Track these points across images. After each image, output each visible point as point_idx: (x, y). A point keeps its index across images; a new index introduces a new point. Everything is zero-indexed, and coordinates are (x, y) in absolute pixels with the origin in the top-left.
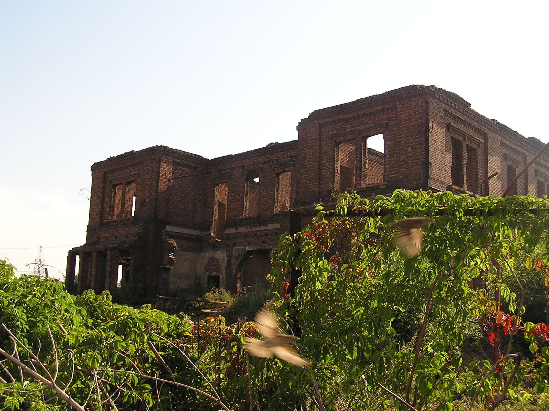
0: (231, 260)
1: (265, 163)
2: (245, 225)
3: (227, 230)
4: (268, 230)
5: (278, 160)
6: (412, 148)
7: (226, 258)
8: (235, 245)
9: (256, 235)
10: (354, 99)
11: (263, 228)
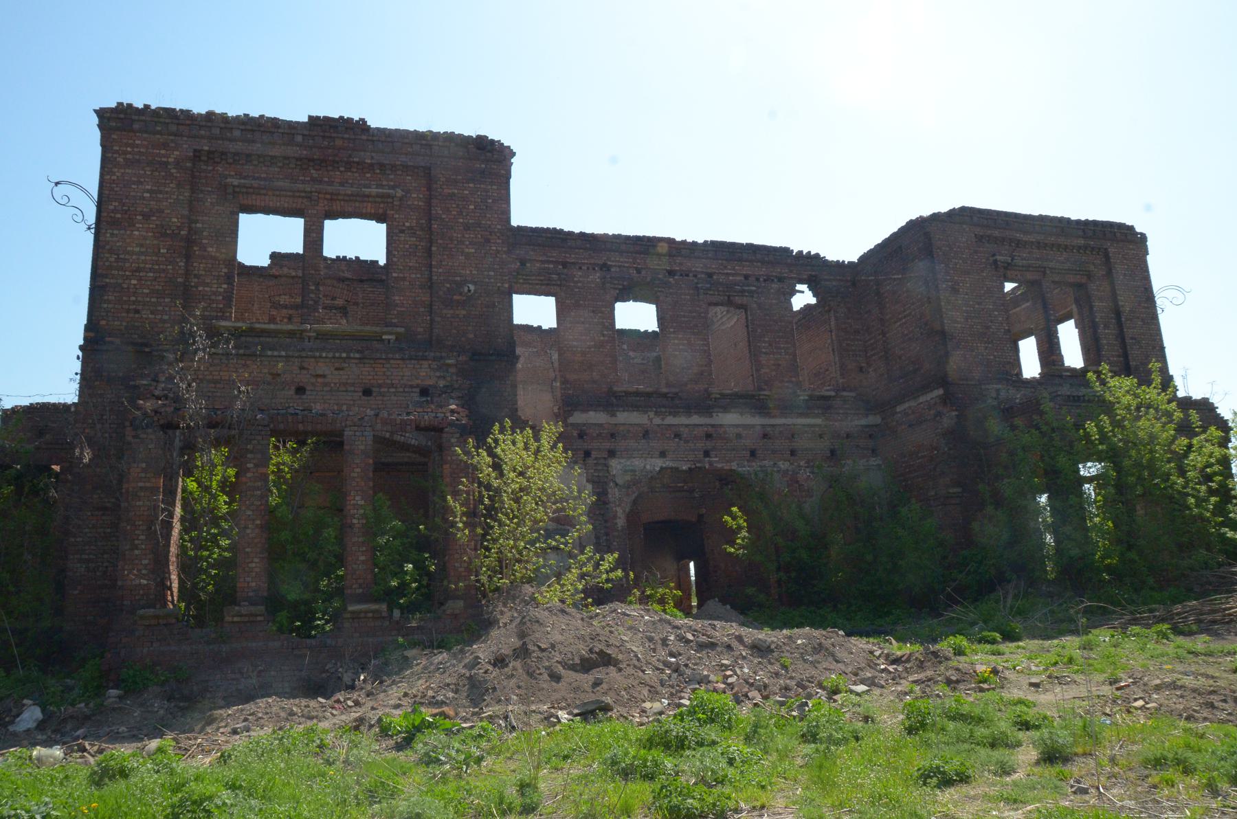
4: (713, 426)
5: (710, 275)
6: (1143, 320)
8: (612, 453)
9: (677, 435)
10: (1036, 212)
11: (696, 419)
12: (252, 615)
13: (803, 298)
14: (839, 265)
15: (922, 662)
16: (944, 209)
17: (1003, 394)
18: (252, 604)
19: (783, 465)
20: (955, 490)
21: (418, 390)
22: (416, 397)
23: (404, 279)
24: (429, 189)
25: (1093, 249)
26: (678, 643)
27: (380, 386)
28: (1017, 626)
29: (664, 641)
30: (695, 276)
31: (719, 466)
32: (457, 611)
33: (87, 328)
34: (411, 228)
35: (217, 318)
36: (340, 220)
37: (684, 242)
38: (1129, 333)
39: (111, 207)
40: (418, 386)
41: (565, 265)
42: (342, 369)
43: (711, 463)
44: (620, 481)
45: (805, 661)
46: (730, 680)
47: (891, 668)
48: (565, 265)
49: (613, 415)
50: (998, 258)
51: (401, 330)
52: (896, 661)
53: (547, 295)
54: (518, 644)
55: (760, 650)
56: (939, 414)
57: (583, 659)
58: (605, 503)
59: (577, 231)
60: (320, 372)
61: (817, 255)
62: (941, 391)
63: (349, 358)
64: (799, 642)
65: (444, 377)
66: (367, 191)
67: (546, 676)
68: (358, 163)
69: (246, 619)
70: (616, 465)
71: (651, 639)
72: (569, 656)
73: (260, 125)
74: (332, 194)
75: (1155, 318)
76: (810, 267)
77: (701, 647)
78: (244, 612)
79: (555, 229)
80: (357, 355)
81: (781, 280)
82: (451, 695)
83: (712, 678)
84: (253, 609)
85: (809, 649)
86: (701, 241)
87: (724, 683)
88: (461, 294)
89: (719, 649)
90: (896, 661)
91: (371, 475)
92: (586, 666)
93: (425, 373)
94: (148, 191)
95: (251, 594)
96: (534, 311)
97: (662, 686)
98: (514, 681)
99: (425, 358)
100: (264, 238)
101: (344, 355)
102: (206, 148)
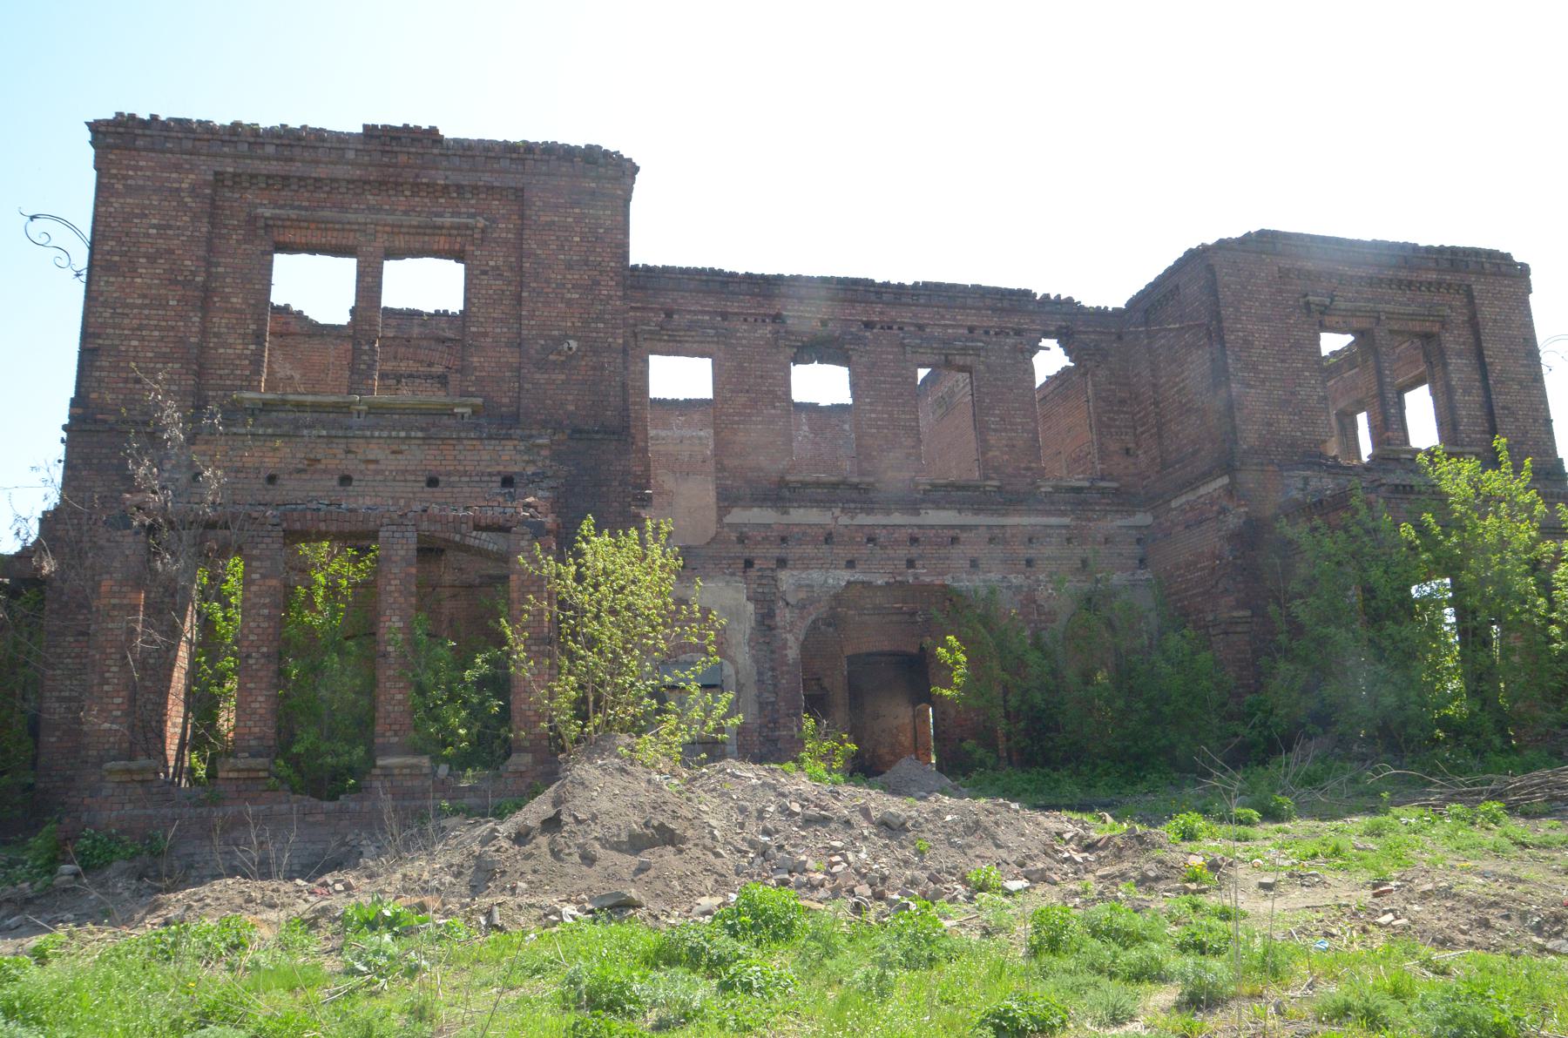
0: (770, 615)
1: (868, 325)
2: (824, 503)
3: (735, 510)
4: (919, 527)
5: (921, 327)
6: (1520, 383)
7: (751, 607)
8: (782, 563)
9: (871, 540)
11: (897, 518)
12: (249, 770)
13: (1050, 360)
14: (1100, 314)
15: (1120, 850)
16: (1237, 233)
17: (1314, 483)
18: (252, 756)
19: (1016, 580)
20: (1241, 613)
21: (499, 479)
22: (496, 487)
23: (485, 335)
24: (522, 217)
25: (1450, 285)
26: (777, 816)
27: (449, 474)
28: (1287, 803)
29: (761, 814)
30: (900, 329)
31: (928, 580)
32: (523, 769)
33: (74, 403)
34: (497, 268)
35: (241, 388)
36: (408, 260)
37: (886, 285)
38: (1499, 400)
39: (107, 248)
40: (499, 473)
41: (725, 316)
42: (400, 452)
43: (916, 577)
44: (792, 600)
45: (952, 844)
46: (836, 869)
47: (1078, 858)
48: (725, 316)
49: (786, 513)
50: (1311, 298)
51: (479, 401)
52: (1090, 847)
53: (702, 356)
54: (552, 812)
55: (890, 827)
56: (1223, 511)
57: (633, 837)
58: (771, 628)
59: (741, 271)
60: (371, 457)
61: (1070, 300)
62: (1225, 480)
63: (408, 438)
64: (949, 818)
65: (534, 462)
66: (438, 220)
67: (576, 858)
68: (427, 185)
69: (245, 775)
70: (786, 578)
71: (742, 810)
72: (615, 830)
73: (300, 139)
74: (393, 226)
75: (1537, 379)
76: (1066, 319)
77: (809, 822)
78: (240, 766)
79: (712, 270)
80: (420, 434)
81: (1018, 333)
82: (448, 879)
83: (811, 864)
84: (253, 762)
85: (960, 828)
86: (909, 282)
87: (827, 873)
88: (559, 353)
89: (833, 826)
90: (1090, 847)
91: (414, 589)
92: (636, 844)
93: (509, 457)
94: (154, 226)
95: (253, 743)
96: (680, 377)
97: (738, 874)
98: (532, 862)
99: (509, 437)
100: (314, 286)
101: (403, 434)
102: (230, 170)
